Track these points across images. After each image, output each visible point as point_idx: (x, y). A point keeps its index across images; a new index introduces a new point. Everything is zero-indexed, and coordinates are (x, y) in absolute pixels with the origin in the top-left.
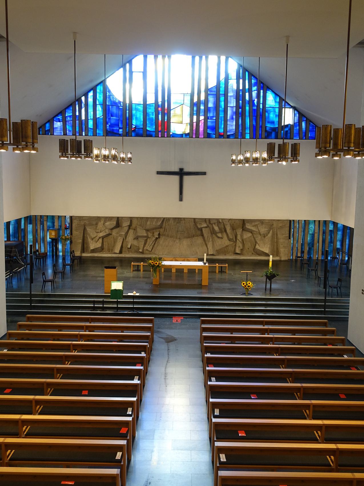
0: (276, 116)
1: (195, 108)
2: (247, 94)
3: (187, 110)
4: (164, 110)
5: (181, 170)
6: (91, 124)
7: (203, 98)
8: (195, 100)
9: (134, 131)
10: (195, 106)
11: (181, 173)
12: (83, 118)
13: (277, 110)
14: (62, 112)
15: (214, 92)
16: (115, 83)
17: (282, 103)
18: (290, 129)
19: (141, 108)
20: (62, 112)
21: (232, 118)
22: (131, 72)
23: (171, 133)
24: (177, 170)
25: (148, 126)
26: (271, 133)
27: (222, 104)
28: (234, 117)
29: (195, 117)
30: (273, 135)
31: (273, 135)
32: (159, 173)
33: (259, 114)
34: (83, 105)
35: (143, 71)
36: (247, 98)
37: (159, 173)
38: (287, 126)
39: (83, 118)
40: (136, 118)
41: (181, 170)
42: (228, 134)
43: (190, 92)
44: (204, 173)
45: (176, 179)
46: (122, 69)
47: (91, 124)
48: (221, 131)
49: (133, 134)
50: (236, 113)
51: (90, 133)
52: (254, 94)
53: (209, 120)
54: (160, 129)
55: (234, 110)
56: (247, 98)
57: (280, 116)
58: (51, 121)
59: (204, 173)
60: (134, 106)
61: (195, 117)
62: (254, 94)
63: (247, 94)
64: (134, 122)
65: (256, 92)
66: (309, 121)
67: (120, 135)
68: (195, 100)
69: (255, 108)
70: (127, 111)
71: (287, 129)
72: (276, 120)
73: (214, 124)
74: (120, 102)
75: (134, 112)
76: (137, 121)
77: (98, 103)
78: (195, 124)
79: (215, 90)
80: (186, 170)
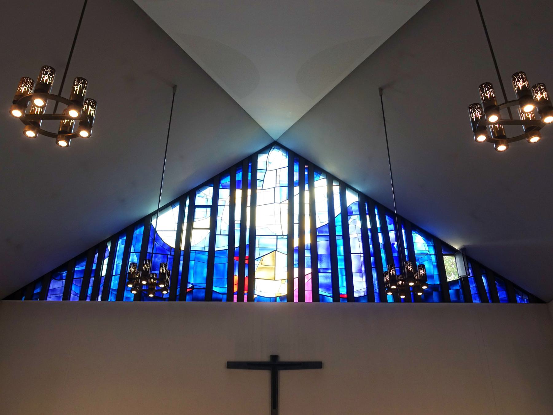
0: (433, 266)
1: (296, 256)
2: (380, 235)
3: (282, 260)
4: (243, 256)
5: (274, 358)
6: (114, 283)
7: (308, 241)
8: (296, 244)
9: (191, 292)
10: (296, 254)
11: (274, 366)
12: (104, 273)
13: (433, 258)
14: (69, 266)
15: (326, 232)
16: (166, 225)
17: (441, 249)
18: (462, 287)
19: (205, 257)
20: (69, 266)
21: (360, 271)
22: (193, 207)
23: (255, 296)
24: (266, 358)
25: (214, 285)
26: (431, 294)
27: (341, 249)
28: (363, 269)
29: (296, 271)
30: (435, 295)
31: (435, 295)
32: (231, 365)
33: (405, 258)
34: (107, 254)
35: (210, 203)
36: (381, 240)
37: (231, 365)
38: (454, 283)
39: (104, 273)
40: (195, 273)
41: (274, 358)
42: (356, 295)
43: (286, 232)
44: (318, 365)
45: (265, 375)
46: (177, 208)
47: (114, 283)
48: (343, 290)
49: (187, 297)
50: (366, 262)
51: (112, 298)
52: (392, 235)
53: (319, 274)
54: (236, 289)
55: (362, 259)
56: (381, 240)
57: (440, 266)
58: (44, 281)
59: (318, 365)
60: (192, 255)
61: (296, 271)
62: (392, 235)
63: (380, 235)
64: (191, 280)
65: (394, 232)
66: (492, 276)
67: (164, 299)
68: (296, 244)
69: (396, 255)
70: (181, 262)
71: (457, 287)
72: (435, 273)
73: (329, 281)
74: (170, 248)
75: (192, 263)
76: (197, 277)
77: (132, 250)
78: (296, 281)
79: (327, 230)
80: (284, 358)
